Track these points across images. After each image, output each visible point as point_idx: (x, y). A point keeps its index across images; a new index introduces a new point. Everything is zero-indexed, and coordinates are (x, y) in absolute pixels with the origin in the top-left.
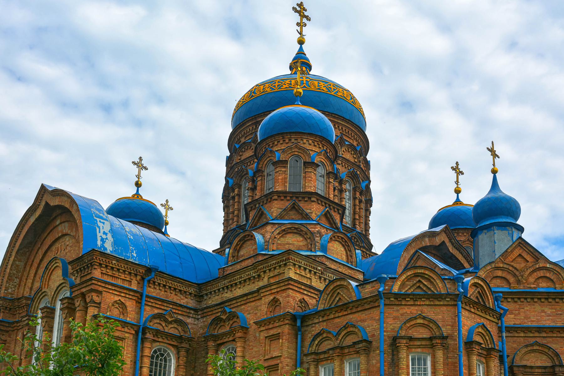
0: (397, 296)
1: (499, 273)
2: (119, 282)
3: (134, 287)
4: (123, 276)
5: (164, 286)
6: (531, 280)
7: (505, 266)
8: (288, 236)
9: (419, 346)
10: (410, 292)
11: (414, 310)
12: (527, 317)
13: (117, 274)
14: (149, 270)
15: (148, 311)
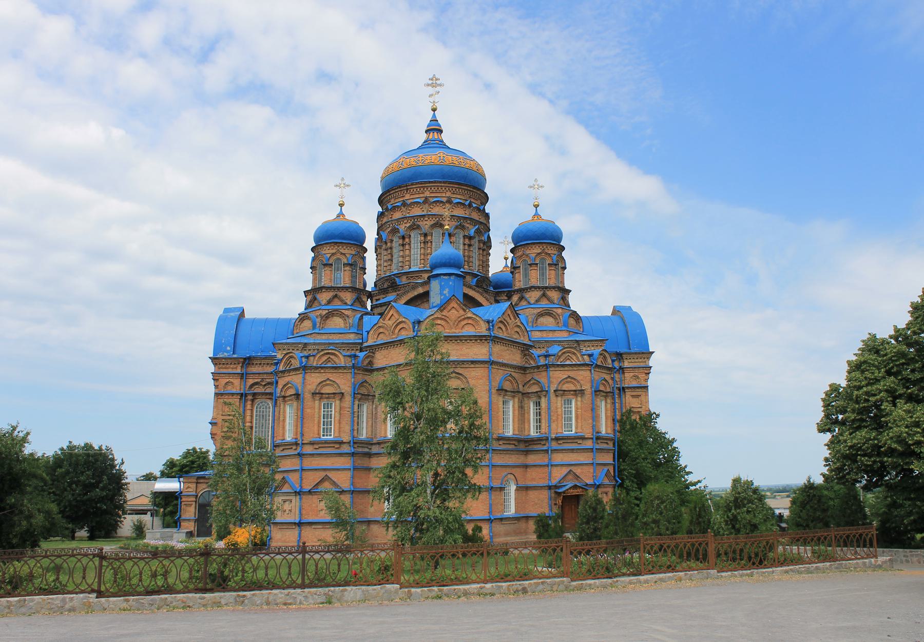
0: (282, 372)
1: (381, 330)
2: (230, 371)
3: (239, 371)
4: (232, 366)
5: (260, 364)
6: (397, 331)
7: (383, 325)
8: (305, 321)
9: (289, 400)
10: (287, 368)
11: (287, 379)
12: (392, 359)
13: (228, 366)
14: (245, 359)
15: (250, 382)
